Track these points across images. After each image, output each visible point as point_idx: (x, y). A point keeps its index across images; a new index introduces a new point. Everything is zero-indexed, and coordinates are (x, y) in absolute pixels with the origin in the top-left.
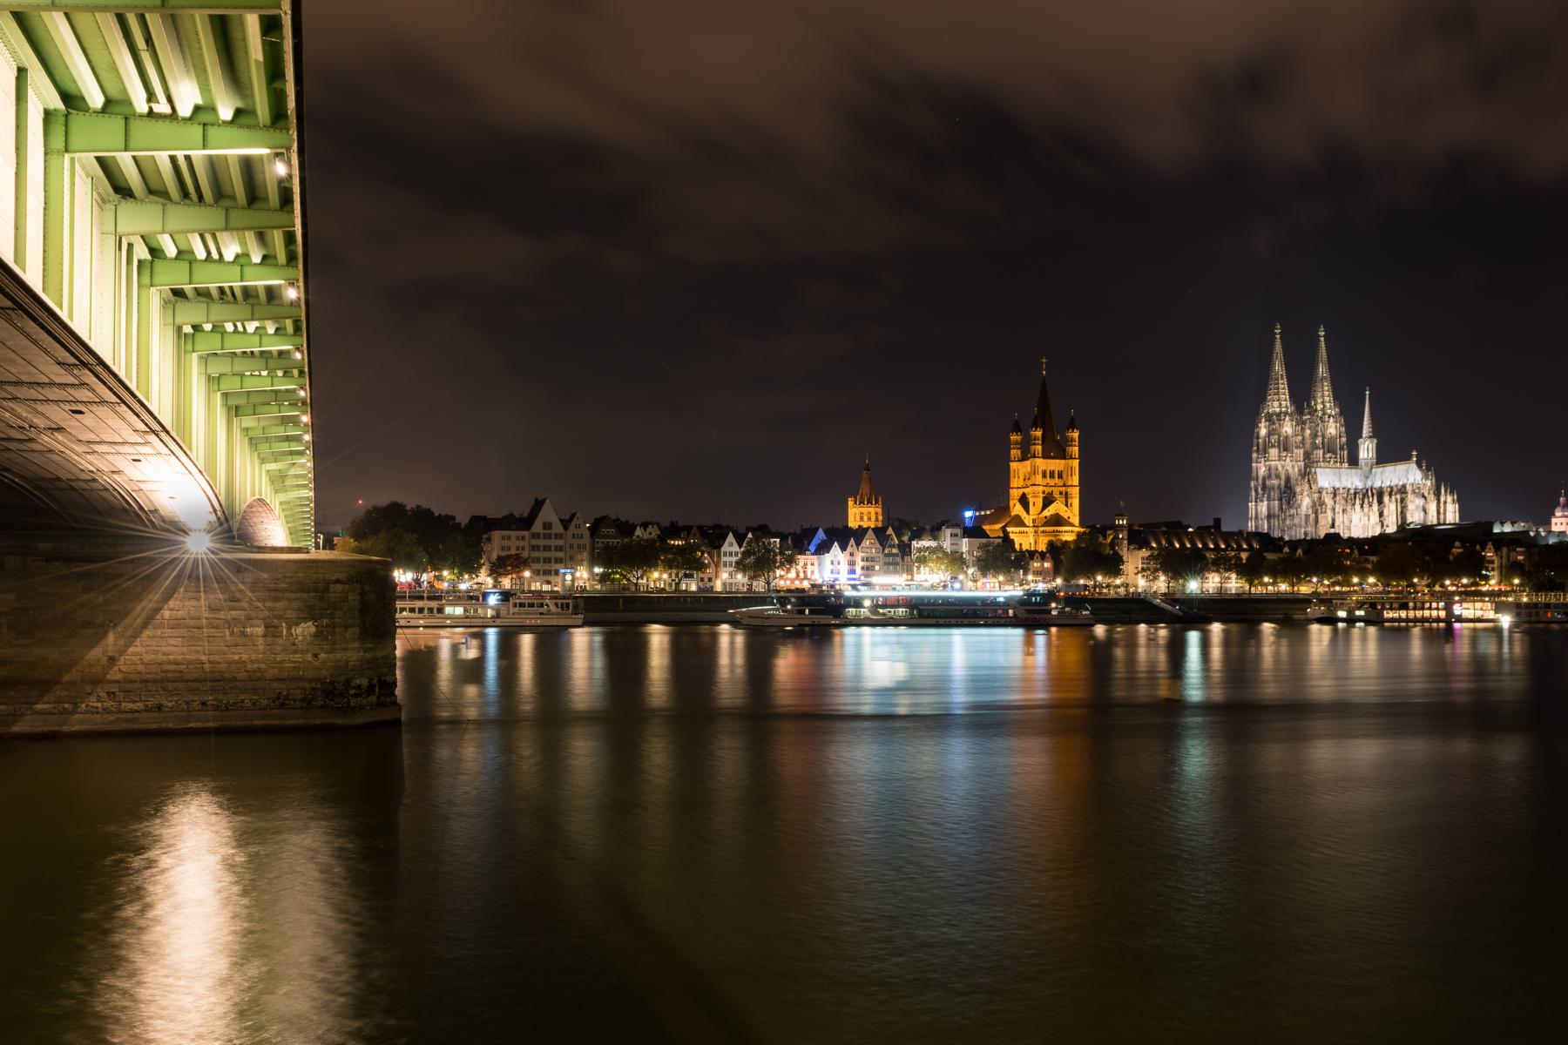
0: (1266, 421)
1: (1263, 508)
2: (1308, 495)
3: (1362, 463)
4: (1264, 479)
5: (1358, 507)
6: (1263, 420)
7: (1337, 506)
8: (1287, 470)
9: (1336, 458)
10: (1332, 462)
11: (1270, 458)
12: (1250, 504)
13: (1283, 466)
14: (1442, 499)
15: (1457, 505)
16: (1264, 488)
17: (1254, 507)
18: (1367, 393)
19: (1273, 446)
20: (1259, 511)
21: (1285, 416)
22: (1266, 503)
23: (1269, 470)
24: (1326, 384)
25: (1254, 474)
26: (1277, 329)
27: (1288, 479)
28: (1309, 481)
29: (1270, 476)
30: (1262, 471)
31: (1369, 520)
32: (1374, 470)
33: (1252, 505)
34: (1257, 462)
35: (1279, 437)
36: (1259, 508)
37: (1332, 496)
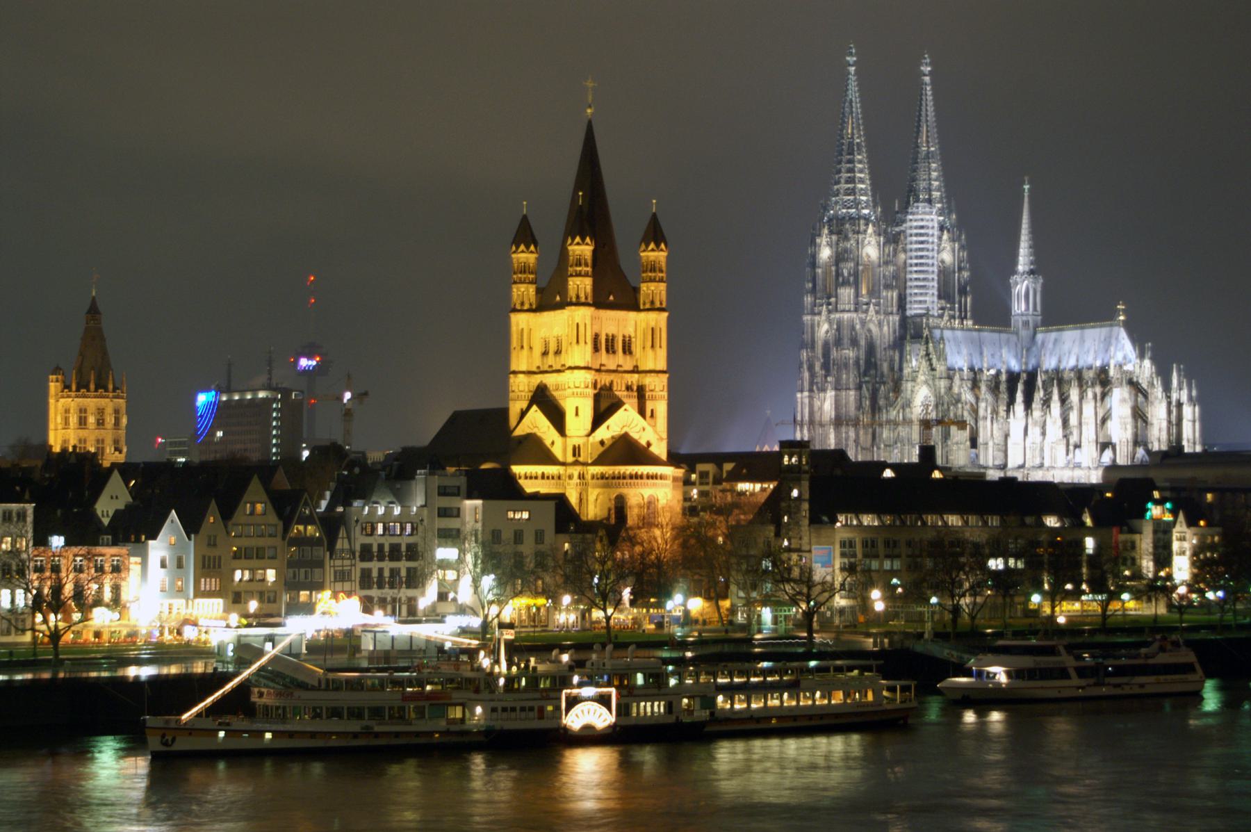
0: (831, 232)
1: (827, 404)
2: (926, 382)
3: (1017, 321)
4: (826, 346)
5: (1019, 407)
6: (826, 231)
7: (982, 405)
8: (869, 331)
9: (952, 309)
10: (946, 318)
11: (840, 307)
12: (799, 395)
13: (863, 323)
14: (1174, 396)
15: (1197, 409)
16: (826, 366)
17: (806, 401)
18: (1026, 187)
19: (846, 283)
20: (816, 408)
21: (867, 225)
22: (830, 394)
23: (838, 329)
24: (934, 165)
25: (807, 337)
26: (851, 54)
27: (871, 348)
28: (928, 354)
29: (838, 342)
30: (824, 330)
31: (1044, 434)
32: (1039, 337)
33: (802, 397)
34: (813, 313)
35: (857, 264)
36: (817, 403)
37: (969, 384)
